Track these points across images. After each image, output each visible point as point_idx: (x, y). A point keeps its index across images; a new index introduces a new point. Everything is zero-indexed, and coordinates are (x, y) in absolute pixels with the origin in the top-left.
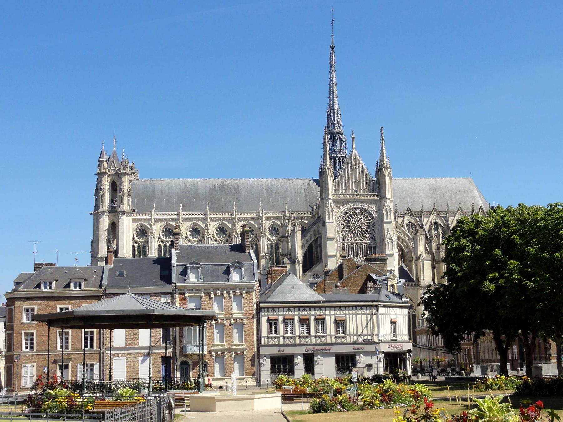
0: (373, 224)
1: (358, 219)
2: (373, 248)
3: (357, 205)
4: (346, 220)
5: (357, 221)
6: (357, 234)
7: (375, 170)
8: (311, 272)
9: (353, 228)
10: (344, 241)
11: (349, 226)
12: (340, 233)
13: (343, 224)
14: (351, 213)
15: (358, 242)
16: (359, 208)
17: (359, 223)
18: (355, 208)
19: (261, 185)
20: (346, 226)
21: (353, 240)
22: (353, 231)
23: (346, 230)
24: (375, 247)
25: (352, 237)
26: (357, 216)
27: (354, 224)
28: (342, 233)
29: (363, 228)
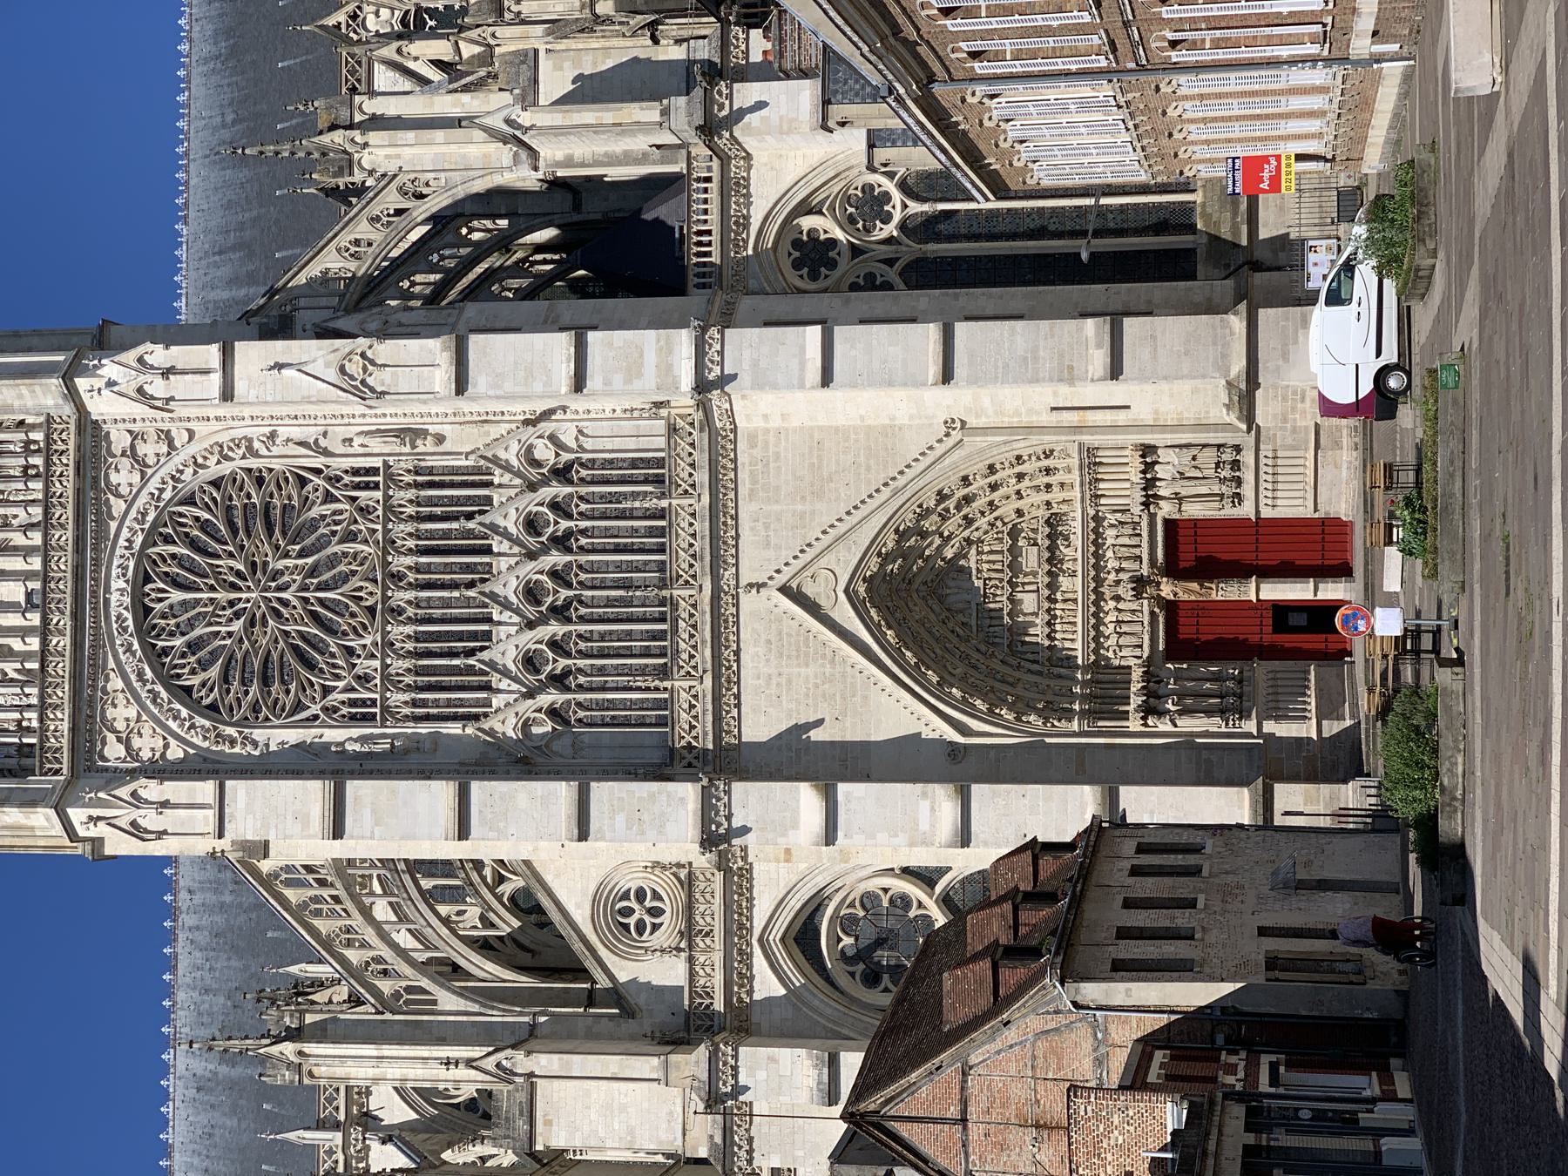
0: (260, 481)
4: (225, 678)
5: (232, 603)
6: (321, 602)
9: (287, 633)
10: (373, 703)
13: (255, 708)
14: (178, 642)
15: (385, 599)
17: (250, 596)
18: (142, 611)
19: (199, 1089)
20: (266, 681)
21: (368, 640)
23: (293, 687)
26: (197, 602)
27: (252, 623)
29: (286, 555)
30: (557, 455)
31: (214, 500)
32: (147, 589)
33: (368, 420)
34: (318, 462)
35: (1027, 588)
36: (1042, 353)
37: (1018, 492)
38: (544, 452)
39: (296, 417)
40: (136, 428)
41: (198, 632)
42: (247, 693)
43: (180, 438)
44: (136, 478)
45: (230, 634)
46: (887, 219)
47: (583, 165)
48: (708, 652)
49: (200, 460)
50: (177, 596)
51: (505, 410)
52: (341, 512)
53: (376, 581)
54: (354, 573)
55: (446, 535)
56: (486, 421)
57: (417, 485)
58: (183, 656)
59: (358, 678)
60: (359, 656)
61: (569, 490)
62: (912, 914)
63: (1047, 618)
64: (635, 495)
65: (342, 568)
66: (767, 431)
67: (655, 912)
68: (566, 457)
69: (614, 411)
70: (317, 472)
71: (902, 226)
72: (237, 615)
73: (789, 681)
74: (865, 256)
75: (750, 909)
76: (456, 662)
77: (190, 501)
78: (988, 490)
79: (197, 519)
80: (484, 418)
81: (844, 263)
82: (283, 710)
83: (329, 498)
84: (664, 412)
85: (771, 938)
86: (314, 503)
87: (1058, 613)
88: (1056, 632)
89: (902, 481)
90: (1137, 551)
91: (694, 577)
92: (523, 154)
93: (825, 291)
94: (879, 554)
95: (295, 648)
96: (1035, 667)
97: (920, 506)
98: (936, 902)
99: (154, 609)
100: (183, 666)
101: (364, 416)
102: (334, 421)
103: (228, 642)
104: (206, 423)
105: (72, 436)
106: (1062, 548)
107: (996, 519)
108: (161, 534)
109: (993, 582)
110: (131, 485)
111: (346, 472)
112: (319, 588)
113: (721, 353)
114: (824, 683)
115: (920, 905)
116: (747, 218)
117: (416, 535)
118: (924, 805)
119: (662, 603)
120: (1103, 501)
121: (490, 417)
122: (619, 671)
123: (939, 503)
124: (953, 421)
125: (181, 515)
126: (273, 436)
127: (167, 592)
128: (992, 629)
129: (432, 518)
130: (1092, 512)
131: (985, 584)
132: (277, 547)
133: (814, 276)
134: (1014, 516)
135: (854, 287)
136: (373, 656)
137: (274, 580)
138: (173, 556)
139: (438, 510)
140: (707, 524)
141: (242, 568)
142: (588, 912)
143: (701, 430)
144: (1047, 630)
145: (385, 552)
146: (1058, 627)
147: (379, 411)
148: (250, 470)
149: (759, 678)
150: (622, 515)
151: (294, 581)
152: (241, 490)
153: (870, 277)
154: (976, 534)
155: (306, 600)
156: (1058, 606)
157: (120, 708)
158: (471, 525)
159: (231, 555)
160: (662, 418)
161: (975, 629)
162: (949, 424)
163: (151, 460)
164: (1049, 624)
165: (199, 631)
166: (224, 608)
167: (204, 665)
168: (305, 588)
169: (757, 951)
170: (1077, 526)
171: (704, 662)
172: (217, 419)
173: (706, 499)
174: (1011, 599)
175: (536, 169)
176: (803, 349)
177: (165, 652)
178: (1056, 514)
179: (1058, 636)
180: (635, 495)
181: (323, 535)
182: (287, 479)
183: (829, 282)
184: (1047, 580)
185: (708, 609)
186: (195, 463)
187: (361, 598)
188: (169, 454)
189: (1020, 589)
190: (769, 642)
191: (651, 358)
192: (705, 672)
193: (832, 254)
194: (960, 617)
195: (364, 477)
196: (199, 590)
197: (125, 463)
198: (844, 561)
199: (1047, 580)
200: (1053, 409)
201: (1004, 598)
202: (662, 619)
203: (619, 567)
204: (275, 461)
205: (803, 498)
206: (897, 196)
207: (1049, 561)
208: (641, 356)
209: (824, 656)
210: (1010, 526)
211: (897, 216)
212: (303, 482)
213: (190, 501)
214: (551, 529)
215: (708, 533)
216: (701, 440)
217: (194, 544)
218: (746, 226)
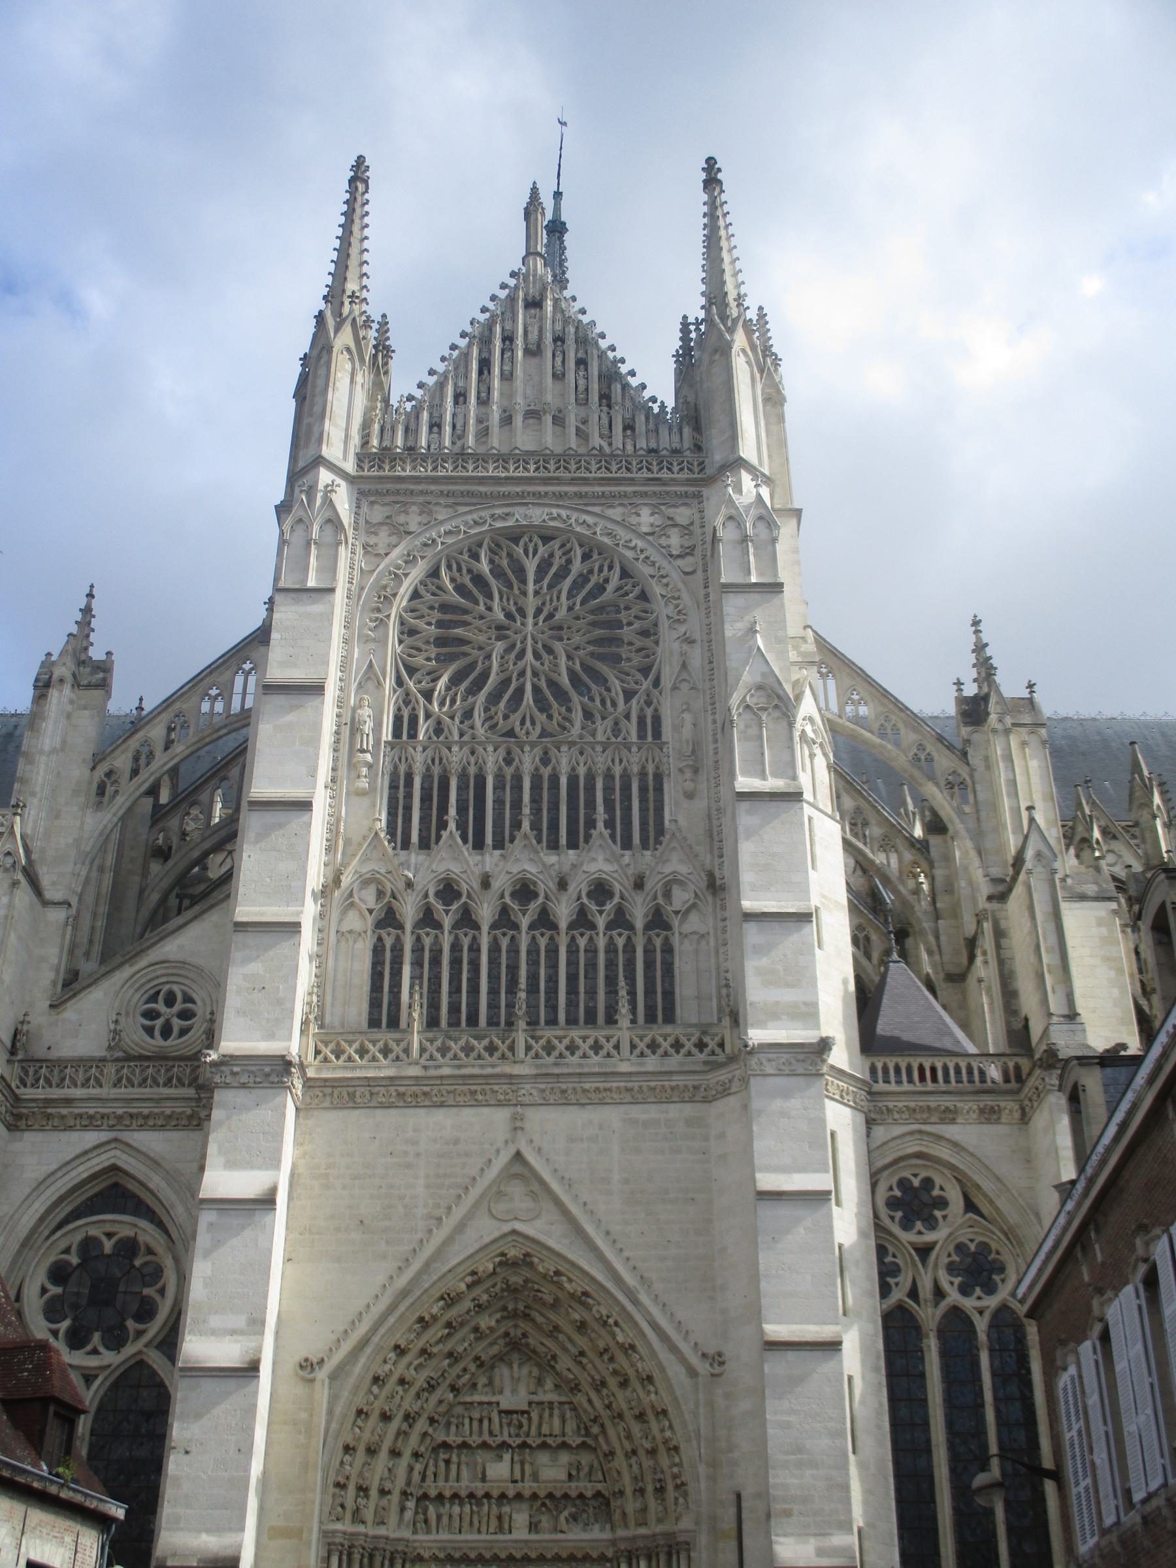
0: (645, 633)
1: (531, 604)
2: (643, 790)
3: (537, 515)
4: (445, 608)
5: (522, 612)
6: (520, 691)
7: (671, 366)
8: (127, 971)
10: (413, 735)
11: (462, 642)
12: (389, 683)
13: (412, 632)
14: (484, 567)
16: (546, 539)
21: (480, 731)
22: (484, 676)
24: (659, 778)
25: (478, 717)
26: (524, 581)
27: (500, 628)
28: (400, 682)
29: (569, 657)
30: (677, 913)
31: (627, 594)
32: (536, 538)
33: (710, 726)
34: (667, 682)
35: (517, 1467)
36: (808, 1472)
38: (680, 898)
39: (711, 662)
40: (696, 528)
41: (493, 582)
42: (429, 624)
43: (686, 563)
44: (645, 529)
45: (489, 609)
46: (965, 1290)
47: (998, 946)
48: (446, 1071)
49: (665, 581)
50: (531, 566)
51: (725, 858)
52: (614, 704)
53: (541, 736)
54: (550, 717)
55: (591, 804)
56: (711, 836)
57: (643, 774)
58: (469, 571)
59: (439, 723)
60: (462, 722)
61: (639, 924)
62: (131, 1324)
63: (480, 1493)
64: (632, 993)
65: (555, 705)
66: (706, 1138)
67: (166, 1032)
68: (675, 922)
69: (727, 971)
70: (657, 683)
71: (956, 1310)
72: (509, 616)
73: (409, 1166)
74: (920, 1266)
75: (154, 1128)
76: (452, 811)
77: (625, 574)
78: (637, 1412)
79: (607, 581)
80: (716, 838)
81: (907, 1237)
82: (410, 655)
83: (629, 695)
84: (727, 1021)
85: (118, 1153)
86: (622, 681)
87: (486, 1508)
88: (461, 1505)
89: (644, 1298)
91: (537, 1056)
92: (1001, 888)
93: (876, 1216)
94: (557, 1273)
95: (472, 666)
96: (416, 1477)
97: (616, 1324)
98: (140, 1352)
99: (517, 545)
100: (459, 570)
101: (714, 722)
102: (708, 697)
103: (482, 608)
104: (702, 586)
105: (686, 476)
107: (602, 1426)
108: (591, 551)
109: (525, 1422)
110: (639, 524)
111: (656, 710)
112: (536, 689)
113: (793, 1074)
114: (405, 1206)
115: (140, 1334)
116: (953, 1121)
117: (591, 778)
118: (240, 1321)
119: (510, 1024)
121: (716, 845)
122: (435, 981)
123: (621, 1346)
124: (722, 1364)
125: (611, 568)
126: (691, 642)
127: (535, 552)
128: (467, 1421)
129: (609, 790)
132: (577, 648)
133: (892, 1204)
134: (605, 1448)
135: (881, 1250)
136: (462, 735)
137: (544, 646)
138: (569, 561)
139: (617, 796)
140: (597, 1070)
141: (558, 616)
142: (172, 957)
143: (705, 1063)
144: (463, 1494)
145: (572, 744)
146: (467, 1508)
147: (719, 736)
148: (656, 625)
149: (415, 1130)
150: (611, 981)
151: (542, 664)
152: (636, 617)
153: (894, 1270)
155: (522, 674)
157: (419, 519)
158: (600, 825)
159: (570, 609)
160: (720, 1020)
162: (718, 1359)
163: (663, 541)
164: (471, 1496)
165: (494, 584)
166: (516, 604)
167: (460, 589)
168: (535, 674)
169: (104, 1136)
171: (437, 1067)
172: (707, 595)
173: (624, 1067)
174: (504, 1445)
175: (990, 898)
176: (803, 1169)
177: (475, 557)
180: (632, 993)
181: (589, 690)
182: (648, 656)
183: (887, 1222)
184: (527, 1493)
185: (497, 1070)
186: (663, 577)
187: (523, 723)
188: (671, 556)
190: (456, 1142)
191: (787, 996)
192: (425, 1068)
193: (919, 1225)
194: (482, 1380)
195: (652, 727)
196: (536, 582)
197: (657, 520)
198: (554, 1237)
199: (527, 1493)
200: (739, 1497)
201: (506, 1438)
202: (493, 1022)
203: (553, 980)
204: (669, 644)
205: (626, 1181)
206: (992, 1302)
207: (550, 1496)
208: (788, 986)
209: (438, 1206)
211: (969, 1304)
212: (645, 671)
213: (625, 574)
214: (594, 908)
215: (586, 1070)
216: (693, 1063)
217: (583, 579)
218: (942, 1121)
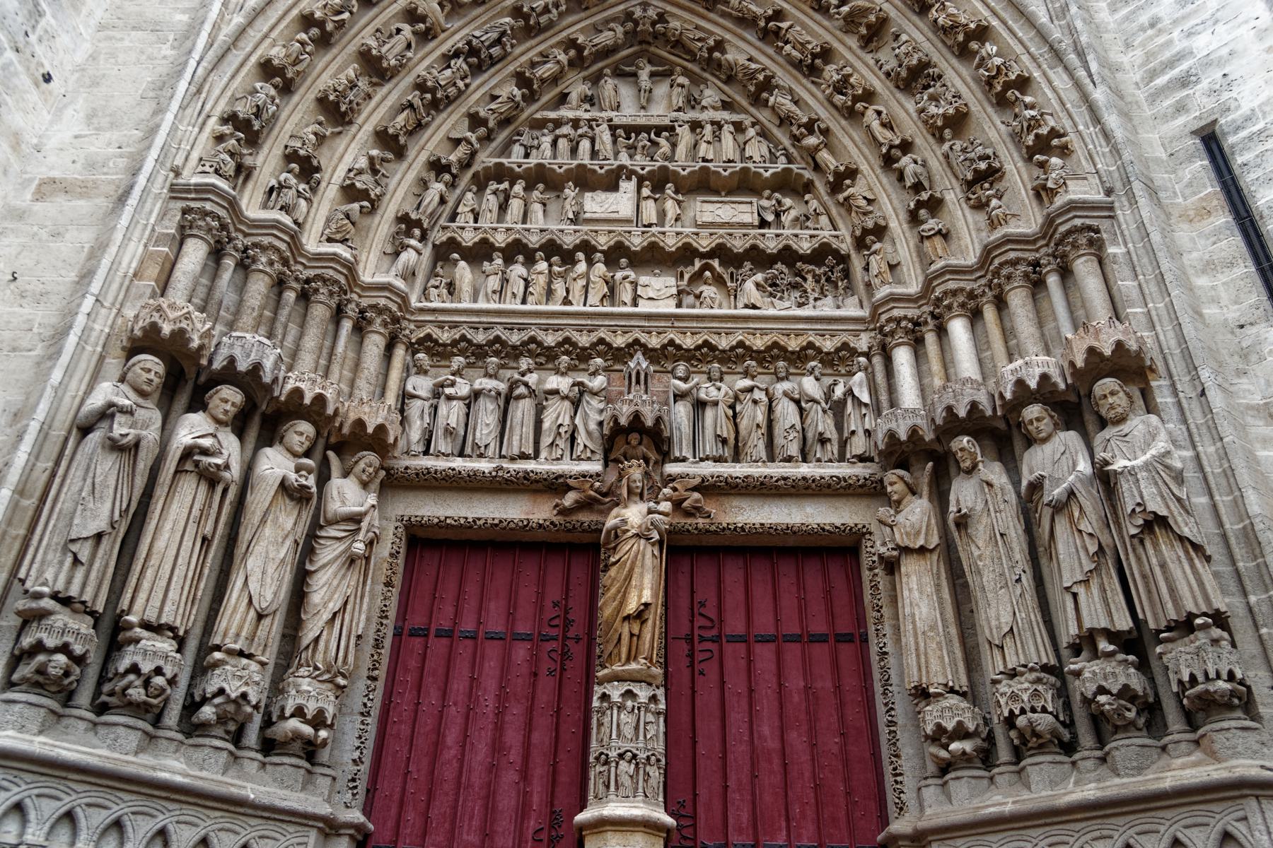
37: (906, 147)
87: (582, 267)
90: (757, 446)
106: (759, 277)
107: (826, 132)
120: (903, 357)
130: (863, 343)
131: (659, 130)
144: (534, 240)
154: (780, 100)
156: (600, 268)
161: (552, 115)
170: (826, 308)
178: (847, 274)
179: (518, 270)
189: (646, 192)
210: (808, 174)
